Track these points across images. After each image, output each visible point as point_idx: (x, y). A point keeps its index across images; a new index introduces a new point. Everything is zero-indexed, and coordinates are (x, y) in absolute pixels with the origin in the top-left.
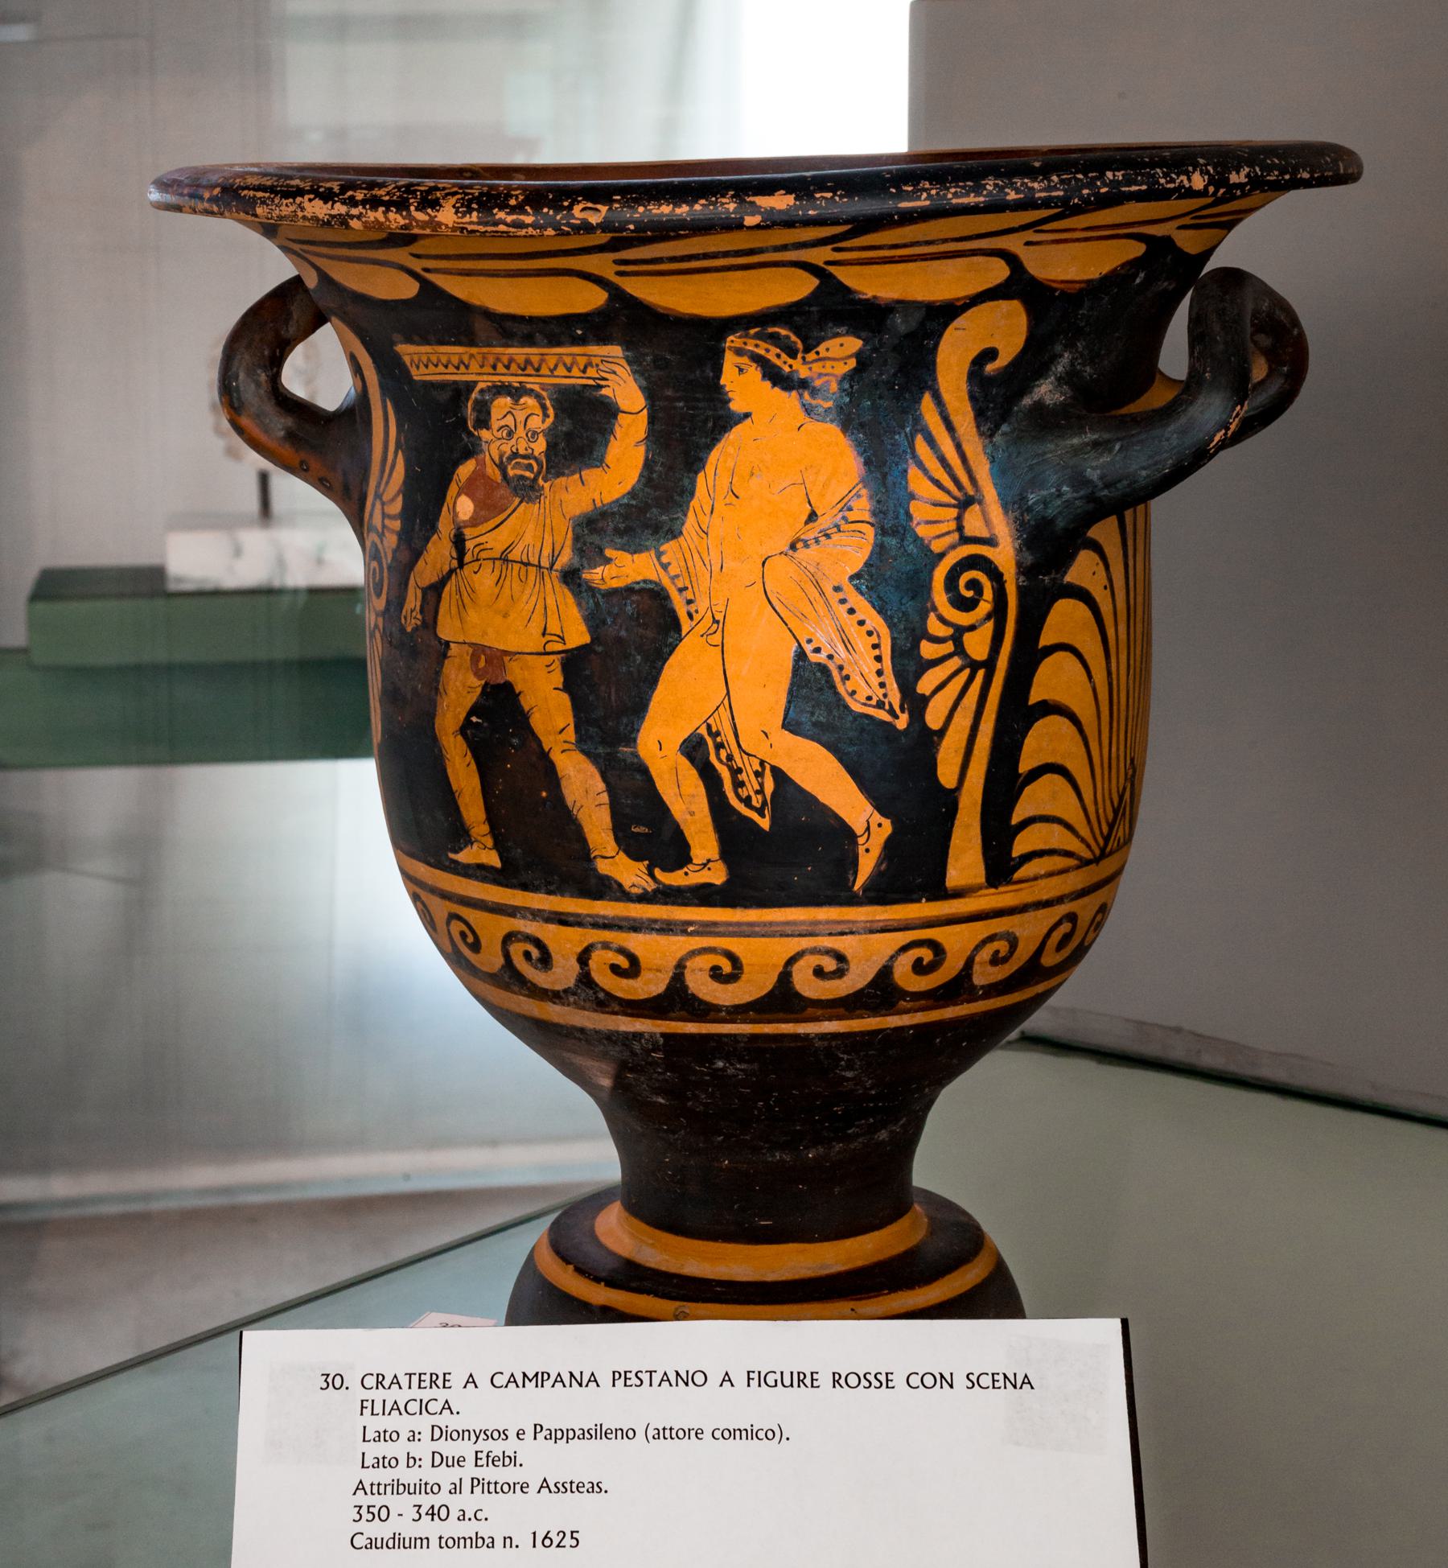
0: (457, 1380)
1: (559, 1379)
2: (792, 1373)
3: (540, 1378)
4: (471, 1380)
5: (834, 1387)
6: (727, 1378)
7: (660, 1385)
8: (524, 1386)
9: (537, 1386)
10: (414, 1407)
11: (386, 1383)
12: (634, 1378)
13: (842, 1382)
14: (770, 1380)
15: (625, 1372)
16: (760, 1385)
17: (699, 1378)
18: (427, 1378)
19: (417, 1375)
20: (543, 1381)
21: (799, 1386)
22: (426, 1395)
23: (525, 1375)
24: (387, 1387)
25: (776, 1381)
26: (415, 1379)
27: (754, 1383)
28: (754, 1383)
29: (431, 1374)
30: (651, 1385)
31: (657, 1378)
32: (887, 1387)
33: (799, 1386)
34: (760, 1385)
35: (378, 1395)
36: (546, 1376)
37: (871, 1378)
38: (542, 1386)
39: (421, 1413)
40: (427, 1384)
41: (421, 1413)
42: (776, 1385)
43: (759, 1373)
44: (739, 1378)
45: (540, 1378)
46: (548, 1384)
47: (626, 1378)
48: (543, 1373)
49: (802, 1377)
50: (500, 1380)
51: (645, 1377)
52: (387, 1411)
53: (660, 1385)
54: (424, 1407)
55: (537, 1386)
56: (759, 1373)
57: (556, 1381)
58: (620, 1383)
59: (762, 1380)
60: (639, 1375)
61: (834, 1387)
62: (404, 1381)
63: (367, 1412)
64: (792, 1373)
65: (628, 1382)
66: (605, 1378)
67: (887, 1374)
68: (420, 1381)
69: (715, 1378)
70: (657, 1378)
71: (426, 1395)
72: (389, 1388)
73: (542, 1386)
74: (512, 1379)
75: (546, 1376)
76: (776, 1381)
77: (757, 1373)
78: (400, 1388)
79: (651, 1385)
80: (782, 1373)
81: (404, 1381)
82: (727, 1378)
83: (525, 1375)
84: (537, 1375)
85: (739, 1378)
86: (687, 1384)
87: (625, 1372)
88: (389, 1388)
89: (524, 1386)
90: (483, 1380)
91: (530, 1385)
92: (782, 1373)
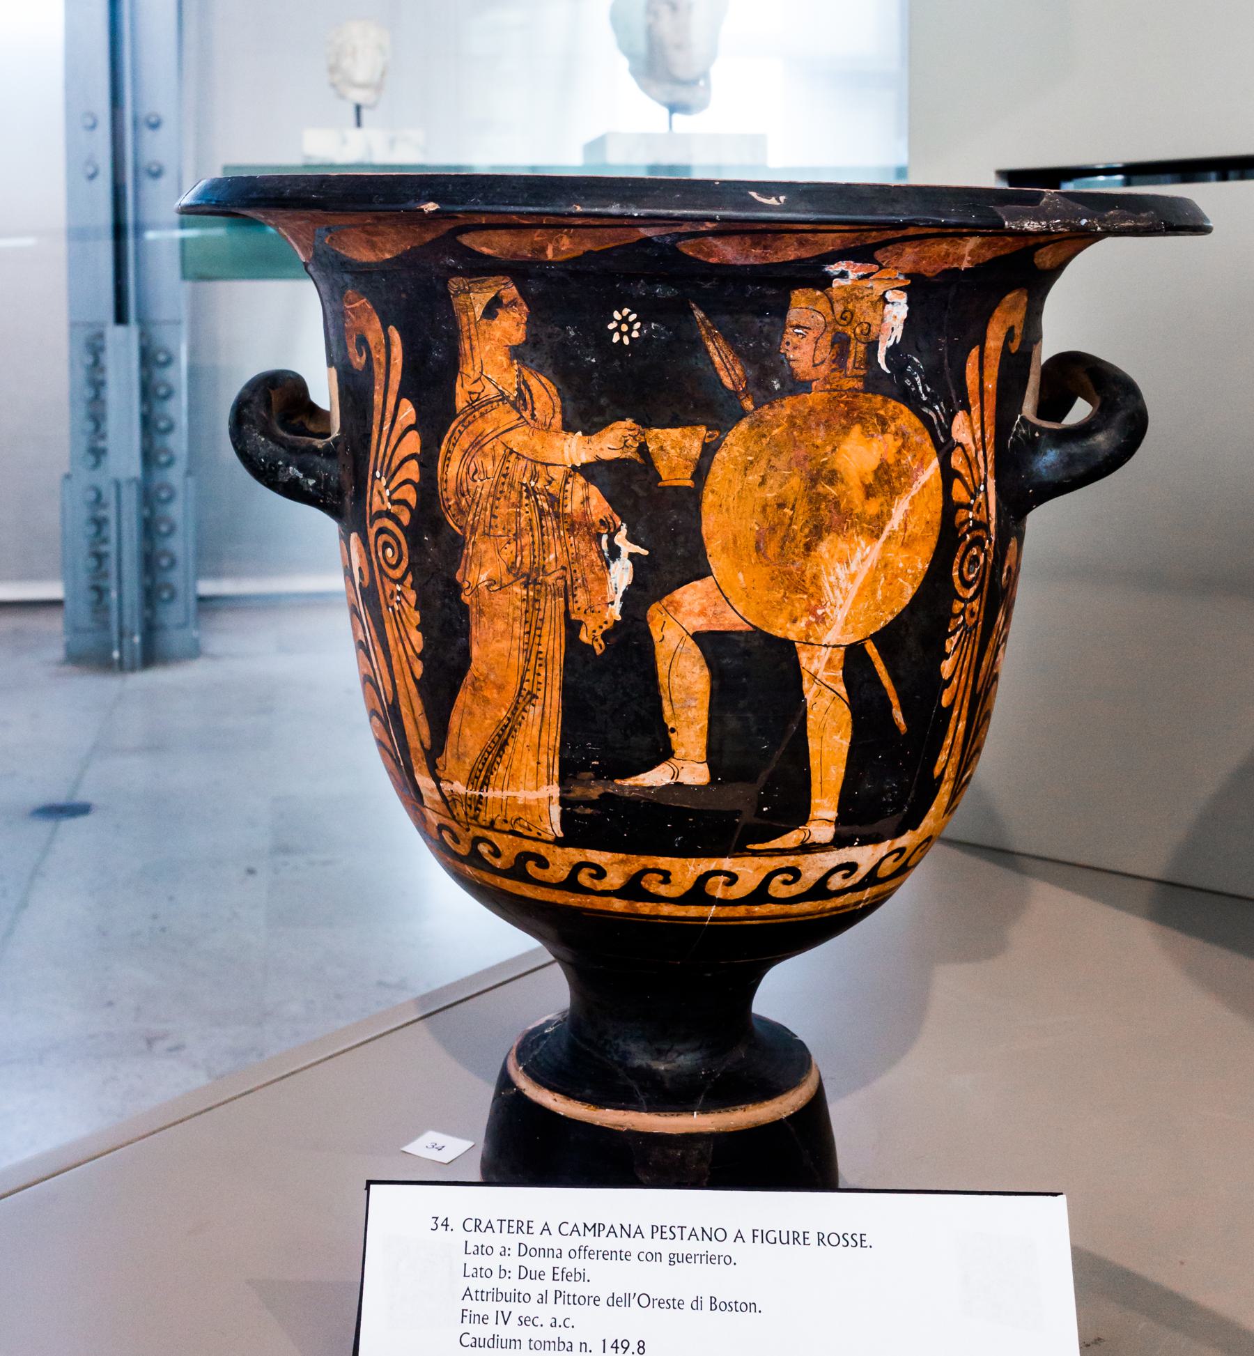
0: (537, 1227)
1: (612, 1230)
4: (546, 1228)
6: (739, 1236)
14: (771, 1237)
17: (720, 1235)
18: (514, 1224)
23: (585, 1226)
26: (505, 1224)
27: (758, 1240)
28: (758, 1240)
31: (687, 1232)
36: (602, 1228)
40: (514, 1229)
44: (748, 1236)
46: (604, 1234)
49: (796, 1235)
51: (677, 1231)
57: (609, 1232)
59: (765, 1237)
60: (673, 1229)
65: (664, 1235)
66: (647, 1231)
68: (509, 1226)
69: (732, 1235)
70: (687, 1232)
74: (575, 1229)
75: (602, 1228)
77: (760, 1232)
82: (739, 1236)
83: (585, 1226)
84: (594, 1226)
85: (748, 1236)
90: (554, 1228)
91: (590, 1234)
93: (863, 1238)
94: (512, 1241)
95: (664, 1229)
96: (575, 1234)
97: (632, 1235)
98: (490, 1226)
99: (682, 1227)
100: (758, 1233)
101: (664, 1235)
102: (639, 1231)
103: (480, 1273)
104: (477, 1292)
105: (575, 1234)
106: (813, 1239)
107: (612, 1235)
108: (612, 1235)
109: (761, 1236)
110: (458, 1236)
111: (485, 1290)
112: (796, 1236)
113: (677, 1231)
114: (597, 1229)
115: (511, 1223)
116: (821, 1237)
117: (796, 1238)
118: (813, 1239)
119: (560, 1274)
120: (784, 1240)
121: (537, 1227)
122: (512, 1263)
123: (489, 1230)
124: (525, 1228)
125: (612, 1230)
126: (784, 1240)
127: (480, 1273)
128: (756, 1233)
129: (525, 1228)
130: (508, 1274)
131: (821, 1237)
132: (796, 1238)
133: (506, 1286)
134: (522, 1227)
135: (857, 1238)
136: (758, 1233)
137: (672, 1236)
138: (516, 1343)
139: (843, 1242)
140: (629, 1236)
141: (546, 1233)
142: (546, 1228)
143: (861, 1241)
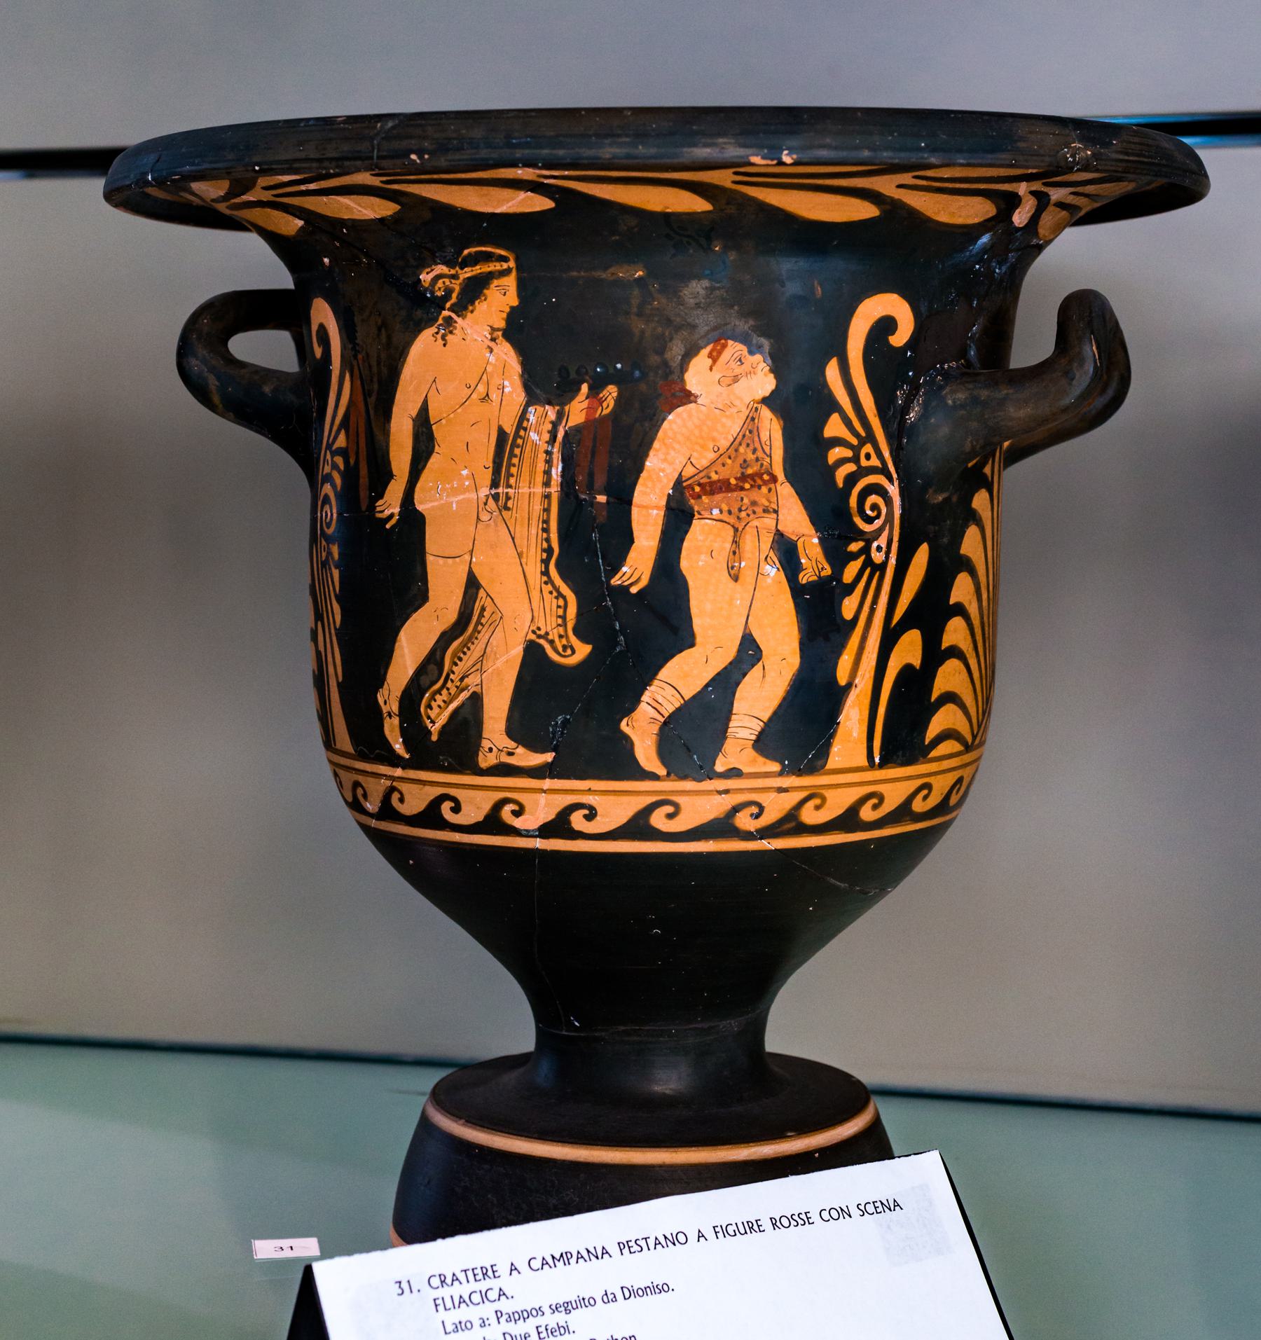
0: (503, 1269)
1: (580, 1256)
2: (743, 1223)
3: (565, 1257)
4: (513, 1268)
5: (774, 1229)
6: (701, 1235)
7: (655, 1248)
8: (555, 1266)
9: (565, 1264)
10: (476, 1298)
11: (449, 1281)
12: (635, 1245)
13: (778, 1224)
14: (731, 1230)
15: (627, 1242)
16: (725, 1237)
17: (681, 1238)
18: (478, 1271)
19: (471, 1271)
20: (568, 1260)
21: (751, 1232)
22: (483, 1286)
23: (553, 1257)
25: (734, 1231)
26: (470, 1274)
27: (720, 1235)
28: (720, 1235)
29: (482, 1268)
30: (649, 1249)
32: (809, 1223)
33: (751, 1232)
34: (725, 1237)
35: (445, 1292)
36: (569, 1256)
37: (796, 1217)
38: (569, 1264)
39: (483, 1302)
40: (480, 1276)
41: (483, 1302)
42: (735, 1235)
43: (721, 1226)
44: (709, 1233)
45: (565, 1257)
46: (573, 1261)
47: (629, 1247)
48: (566, 1253)
49: (751, 1225)
50: (536, 1264)
51: (643, 1243)
52: (457, 1303)
53: (655, 1248)
54: (484, 1296)
55: (565, 1264)
56: (721, 1226)
57: (578, 1258)
58: (626, 1251)
59: (725, 1232)
60: (638, 1242)
61: (774, 1229)
62: (462, 1276)
63: (441, 1308)
64: (743, 1223)
66: (614, 1250)
67: (806, 1213)
68: (475, 1275)
69: (693, 1236)
70: (651, 1242)
71: (483, 1286)
72: (452, 1284)
73: (569, 1264)
74: (544, 1262)
75: (569, 1256)
76: (734, 1231)
77: (719, 1227)
78: (461, 1283)
79: (649, 1249)
80: (736, 1224)
81: (462, 1276)
82: (701, 1235)
83: (553, 1257)
84: (562, 1255)
85: (709, 1233)
86: (674, 1244)
87: (627, 1242)
88: (452, 1284)
89: (555, 1266)
90: (522, 1266)
92: (736, 1224)
93: (809, 1215)
95: (630, 1244)
97: (600, 1256)
98: (455, 1278)
99: (646, 1239)
100: (718, 1229)
101: (632, 1250)
102: (605, 1251)
105: (546, 1267)
106: (766, 1224)
107: (581, 1261)
108: (581, 1261)
109: (722, 1231)
112: (751, 1225)
113: (643, 1243)
115: (476, 1272)
116: (774, 1222)
117: (752, 1227)
118: (766, 1224)
120: (743, 1232)
123: (456, 1283)
124: (490, 1273)
125: (580, 1256)
126: (743, 1232)
128: (717, 1229)
129: (490, 1273)
131: (774, 1222)
132: (752, 1227)
135: (803, 1216)
136: (718, 1229)
137: (640, 1249)
139: (793, 1223)
140: (597, 1258)
141: (514, 1273)
143: (808, 1218)
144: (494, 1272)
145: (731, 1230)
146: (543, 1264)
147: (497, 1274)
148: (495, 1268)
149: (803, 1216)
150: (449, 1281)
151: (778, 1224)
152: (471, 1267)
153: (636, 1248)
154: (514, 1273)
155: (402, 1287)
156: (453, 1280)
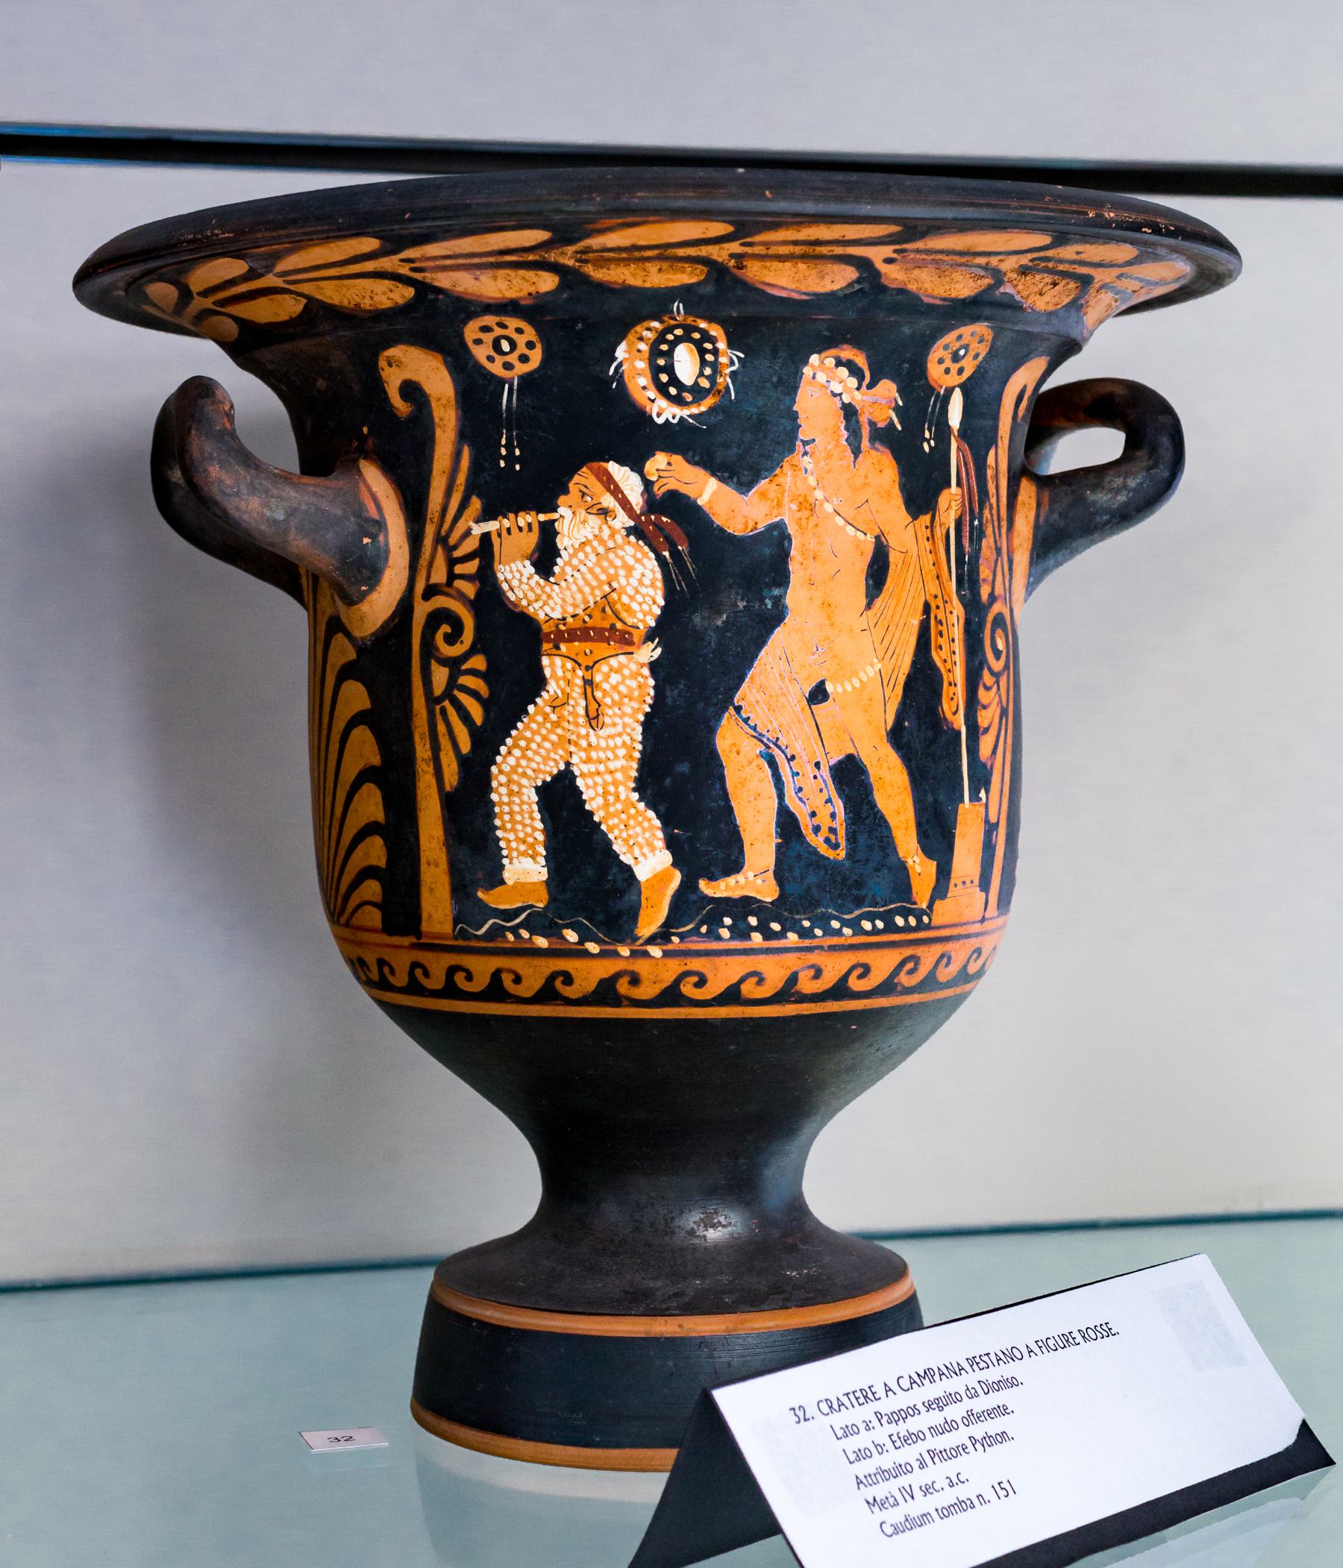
0: (880, 1392)
4: (888, 1390)
11: (835, 1406)
18: (858, 1394)
24: (837, 1409)
29: (861, 1390)
40: (862, 1400)
46: (937, 1377)
51: (985, 1358)
74: (913, 1382)
81: (845, 1400)
84: (925, 1372)
91: (926, 1382)
94: (867, 1411)
96: (914, 1385)
98: (841, 1404)
103: (861, 1455)
104: (865, 1477)
109: (1044, 1345)
110: (821, 1423)
111: (872, 1473)
113: (985, 1358)
114: (928, 1374)
117: (1067, 1340)
119: (898, 1440)
121: (880, 1392)
122: (882, 1433)
127: (861, 1455)
129: (870, 1395)
130: (884, 1448)
132: (1067, 1340)
133: (886, 1461)
134: (866, 1395)
135: (1104, 1327)
136: (1040, 1344)
138: (924, 1519)
142: (888, 1390)
144: (873, 1394)
145: (1051, 1342)
146: (911, 1384)
147: (877, 1396)
148: (873, 1390)
149: (1104, 1327)
150: (835, 1406)
151: (1086, 1336)
152: (850, 1391)
153: (982, 1365)
154: (890, 1393)
155: (800, 1415)
156: (839, 1406)
